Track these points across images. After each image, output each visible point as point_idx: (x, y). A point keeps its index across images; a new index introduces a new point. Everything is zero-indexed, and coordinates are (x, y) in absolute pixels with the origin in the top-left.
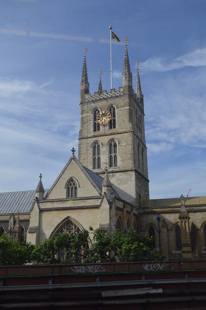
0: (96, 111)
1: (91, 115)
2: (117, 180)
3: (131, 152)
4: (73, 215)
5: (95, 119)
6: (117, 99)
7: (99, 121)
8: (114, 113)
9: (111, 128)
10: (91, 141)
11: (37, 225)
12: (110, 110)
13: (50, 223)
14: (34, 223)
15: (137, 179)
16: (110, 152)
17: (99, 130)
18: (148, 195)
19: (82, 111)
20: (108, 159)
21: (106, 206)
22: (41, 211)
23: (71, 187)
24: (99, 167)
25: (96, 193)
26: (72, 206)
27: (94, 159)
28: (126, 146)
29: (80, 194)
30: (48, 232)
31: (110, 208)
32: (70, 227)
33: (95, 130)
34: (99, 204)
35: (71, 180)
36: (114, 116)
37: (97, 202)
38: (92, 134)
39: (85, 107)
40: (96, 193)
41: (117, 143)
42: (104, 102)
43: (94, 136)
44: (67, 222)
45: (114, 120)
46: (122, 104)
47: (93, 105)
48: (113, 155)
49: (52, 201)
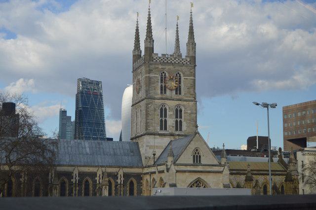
4: (203, 177)
5: (162, 82)
8: (180, 79)
9: (176, 93)
16: (177, 117)
17: (165, 93)
20: (175, 122)
24: (166, 129)
27: (161, 121)
33: (161, 93)
34: (222, 170)
36: (180, 83)
38: (159, 96)
41: (183, 110)
42: (171, 67)
43: (162, 99)
45: (180, 87)
46: (188, 73)
47: (160, 67)
48: (179, 120)
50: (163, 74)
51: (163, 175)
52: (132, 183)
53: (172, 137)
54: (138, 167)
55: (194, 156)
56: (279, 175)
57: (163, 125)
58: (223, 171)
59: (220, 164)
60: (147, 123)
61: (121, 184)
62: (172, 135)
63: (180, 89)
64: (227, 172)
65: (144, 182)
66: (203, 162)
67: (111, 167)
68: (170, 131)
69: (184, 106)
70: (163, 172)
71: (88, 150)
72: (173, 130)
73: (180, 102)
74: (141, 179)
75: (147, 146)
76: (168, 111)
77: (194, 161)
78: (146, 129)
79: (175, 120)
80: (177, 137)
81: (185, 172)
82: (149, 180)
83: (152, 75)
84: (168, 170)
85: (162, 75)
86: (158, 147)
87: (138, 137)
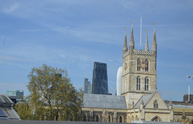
4: (159, 115)
6: (150, 57)
8: (148, 63)
9: (146, 70)
12: (146, 61)
16: (146, 83)
17: (140, 70)
24: (140, 89)
26: (159, 112)
27: (137, 85)
28: (153, 81)
33: (138, 70)
36: (148, 65)
38: (137, 72)
39: (133, 56)
41: (149, 79)
42: (143, 57)
45: (148, 67)
47: (138, 56)
50: (139, 60)
51: (138, 114)
52: (121, 118)
53: (143, 94)
54: (124, 109)
55: (154, 104)
57: (138, 87)
58: (170, 113)
59: (168, 109)
60: (130, 86)
61: (115, 118)
62: (143, 93)
63: (148, 68)
64: (172, 113)
65: (128, 117)
66: (159, 107)
67: (110, 109)
68: (142, 91)
69: (150, 77)
70: (138, 112)
71: (98, 99)
72: (144, 91)
73: (147, 75)
74: (126, 115)
75: (130, 98)
76: (141, 80)
77: (154, 107)
78: (129, 89)
79: (144, 84)
80: (146, 94)
81: (162, 113)
82: (130, 116)
83: (133, 61)
84: (140, 111)
85: (138, 61)
86: (135, 99)
87: (125, 93)
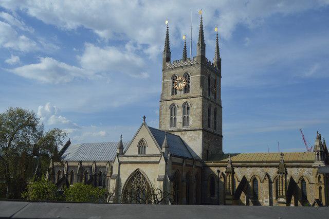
0: (174, 78)
1: (171, 81)
2: (189, 137)
3: (201, 114)
5: (173, 84)
6: (192, 67)
7: (176, 86)
8: (189, 79)
10: (169, 103)
11: (117, 174)
12: (186, 77)
13: (126, 173)
14: (115, 172)
15: (204, 137)
18: (221, 149)
19: (164, 77)
20: (182, 119)
21: (163, 162)
22: (120, 163)
23: (142, 145)
24: (175, 125)
25: (158, 152)
26: (141, 161)
28: (196, 109)
29: (148, 152)
30: (124, 179)
31: (166, 164)
32: (139, 176)
33: (173, 94)
35: (142, 140)
37: (157, 159)
38: (171, 97)
40: (158, 152)
42: (181, 70)
43: (172, 99)
44: (137, 173)
45: (189, 86)
47: (172, 72)
48: (186, 116)
49: (128, 156)
56: (298, 167)
